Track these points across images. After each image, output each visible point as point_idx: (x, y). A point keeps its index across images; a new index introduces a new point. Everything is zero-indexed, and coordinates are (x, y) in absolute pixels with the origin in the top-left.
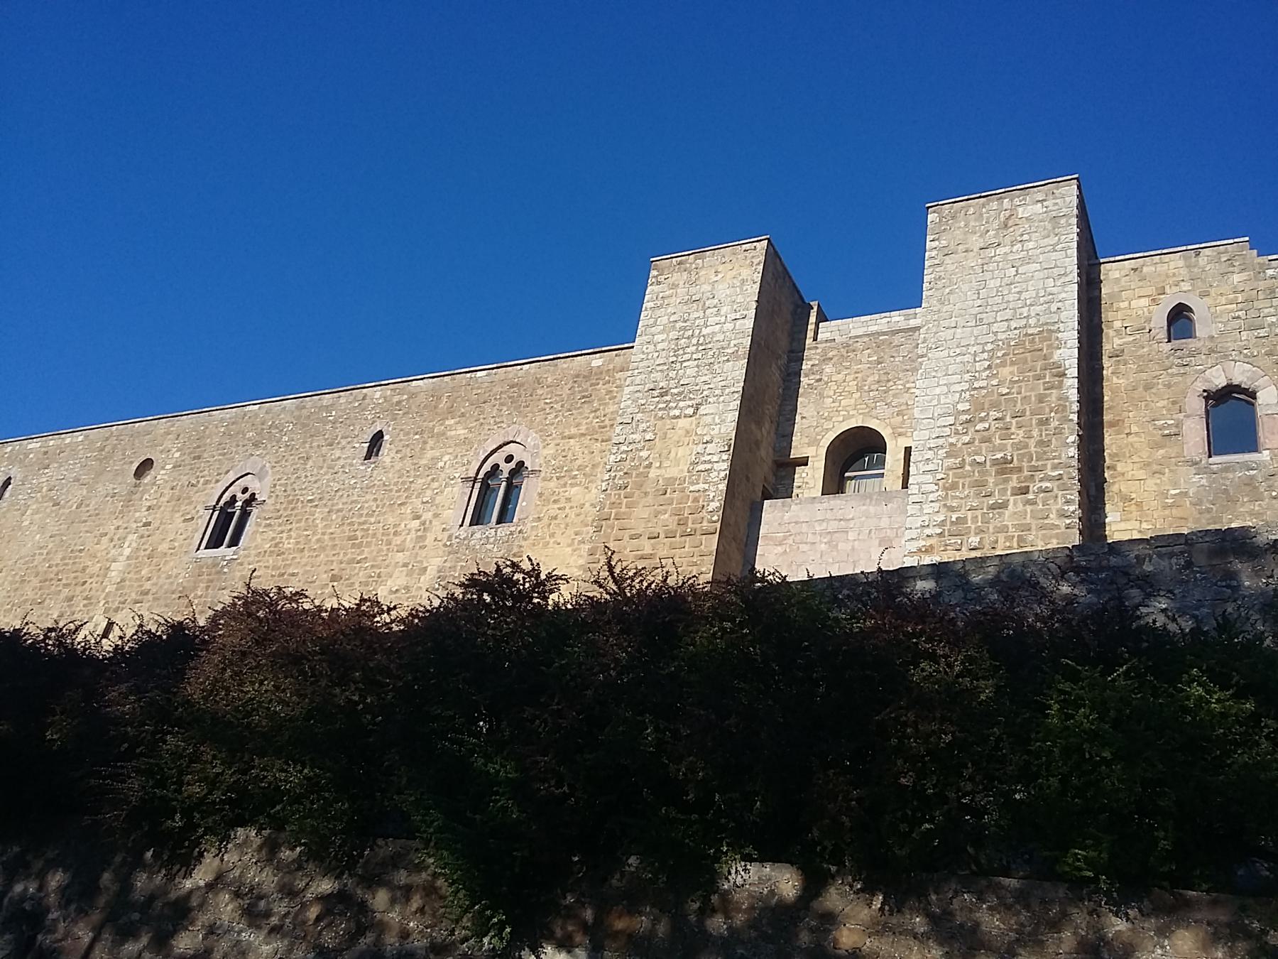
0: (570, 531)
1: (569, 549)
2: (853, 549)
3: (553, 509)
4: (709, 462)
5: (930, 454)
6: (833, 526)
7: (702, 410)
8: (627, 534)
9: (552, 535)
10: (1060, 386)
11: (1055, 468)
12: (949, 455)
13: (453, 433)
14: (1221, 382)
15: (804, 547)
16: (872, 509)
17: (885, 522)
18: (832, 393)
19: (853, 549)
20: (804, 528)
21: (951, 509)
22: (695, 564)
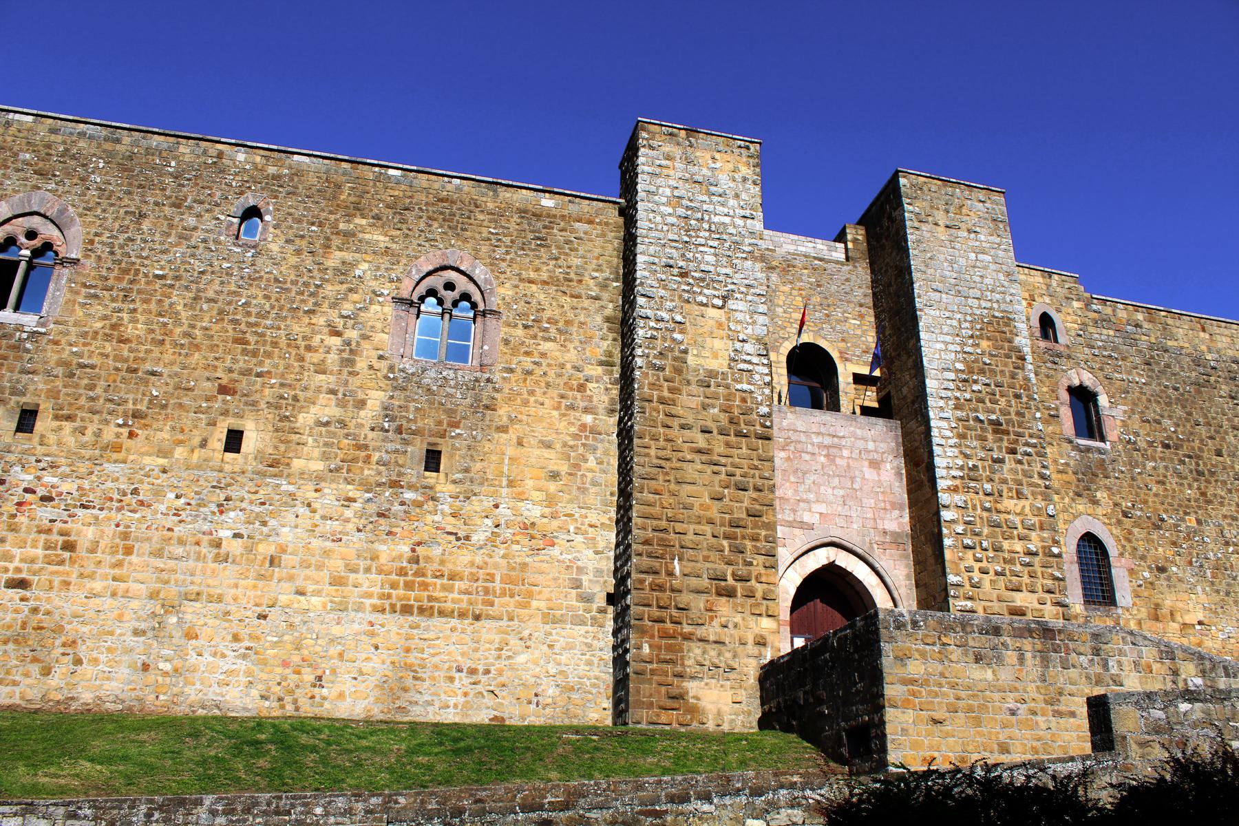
0: (554, 393)
1: (555, 413)
2: (848, 466)
3: (527, 363)
4: (750, 362)
5: (942, 403)
6: (828, 441)
7: (731, 304)
8: (675, 423)
9: (531, 393)
10: (1023, 369)
11: (1031, 436)
12: (957, 407)
13: (367, 236)
14: (1076, 382)
15: (807, 457)
16: (859, 432)
17: (871, 445)
18: (781, 303)
19: (848, 466)
20: (803, 438)
21: (967, 456)
22: (756, 468)
